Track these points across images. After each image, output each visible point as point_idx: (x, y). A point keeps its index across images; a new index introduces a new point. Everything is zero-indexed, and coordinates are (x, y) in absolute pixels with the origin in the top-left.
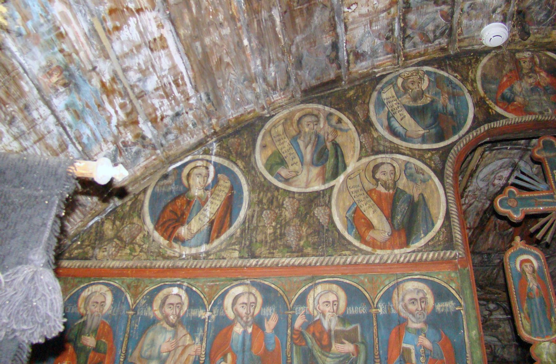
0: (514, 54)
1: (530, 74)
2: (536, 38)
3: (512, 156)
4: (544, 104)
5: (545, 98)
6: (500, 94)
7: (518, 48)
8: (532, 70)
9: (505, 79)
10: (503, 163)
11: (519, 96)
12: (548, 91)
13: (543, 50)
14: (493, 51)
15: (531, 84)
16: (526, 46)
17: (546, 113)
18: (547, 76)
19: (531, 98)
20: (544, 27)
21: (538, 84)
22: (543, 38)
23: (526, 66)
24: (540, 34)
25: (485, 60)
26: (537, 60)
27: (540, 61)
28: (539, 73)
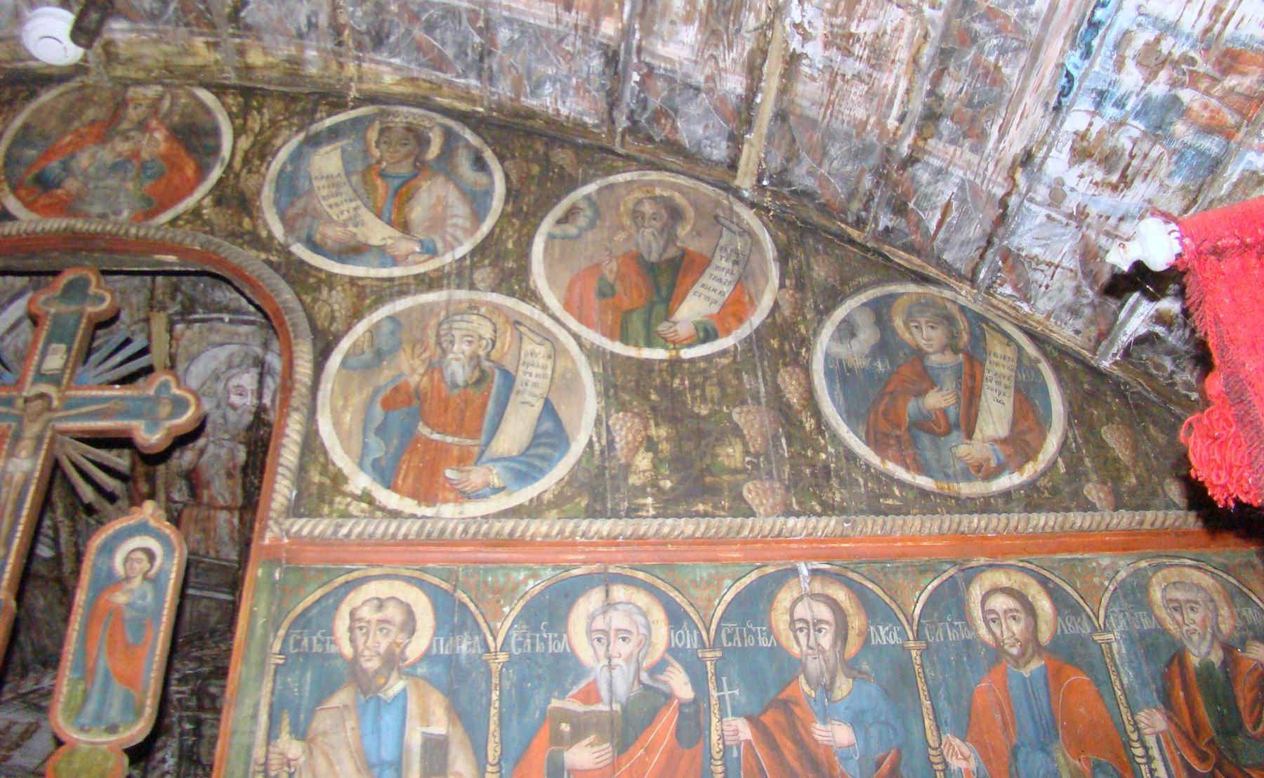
0: (126, 86)
1: (132, 134)
2: (166, 54)
3: (243, 339)
4: (122, 199)
5: (130, 186)
6: (36, 171)
7: (133, 75)
8: (143, 126)
9: (68, 139)
10: (231, 355)
11: (75, 177)
12: (149, 172)
13: (191, 85)
14: (78, 79)
15: (120, 154)
16: (150, 71)
17: (112, 218)
18: (166, 139)
19: (101, 184)
20: (168, 27)
21: (136, 154)
22: (180, 54)
23: (133, 114)
24: (168, 43)
25: (47, 97)
26: (166, 104)
27: (172, 104)
28: (153, 130)
